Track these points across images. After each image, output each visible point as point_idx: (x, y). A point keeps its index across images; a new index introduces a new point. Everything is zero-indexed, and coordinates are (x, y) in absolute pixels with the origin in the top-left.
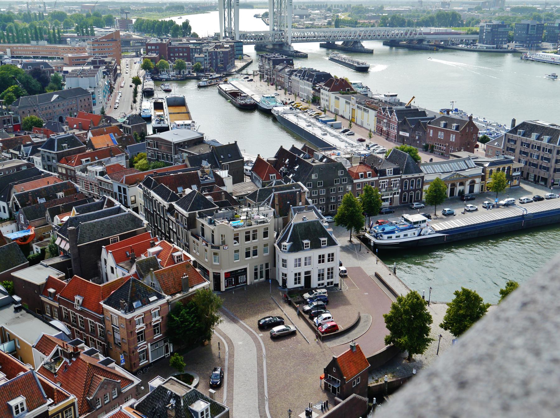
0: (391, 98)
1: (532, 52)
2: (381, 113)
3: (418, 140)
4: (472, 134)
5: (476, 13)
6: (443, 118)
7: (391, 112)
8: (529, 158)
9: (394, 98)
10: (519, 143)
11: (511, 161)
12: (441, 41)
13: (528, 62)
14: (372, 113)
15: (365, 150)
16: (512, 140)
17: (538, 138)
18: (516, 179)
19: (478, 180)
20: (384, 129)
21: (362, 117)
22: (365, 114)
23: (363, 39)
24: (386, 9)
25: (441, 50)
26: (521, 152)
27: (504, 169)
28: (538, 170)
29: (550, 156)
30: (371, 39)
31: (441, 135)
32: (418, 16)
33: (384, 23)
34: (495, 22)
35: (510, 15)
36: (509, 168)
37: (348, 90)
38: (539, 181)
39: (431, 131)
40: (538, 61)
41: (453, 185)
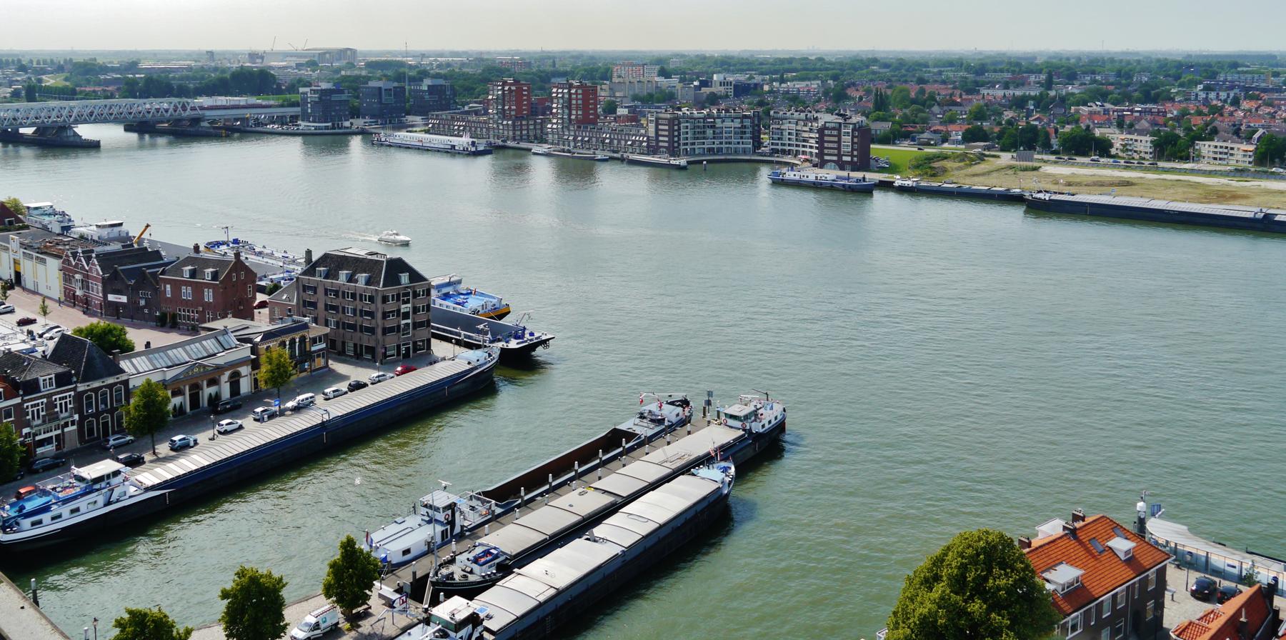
0: (109, 230)
1: (389, 132)
2: (70, 263)
3: (144, 307)
4: (245, 284)
5: (306, 73)
6: (189, 261)
7: (88, 259)
8: (340, 315)
9: (116, 229)
10: (321, 291)
11: (305, 326)
12: (237, 120)
13: (383, 149)
14: (53, 264)
15: (24, 341)
16: (310, 288)
17: (351, 279)
18: (318, 356)
19: (245, 370)
20: (79, 293)
21: (35, 274)
22: (40, 267)
23: (77, 122)
24: (144, 65)
25: (236, 135)
26: (328, 307)
27: (293, 342)
28: (359, 334)
29: (373, 307)
30: (95, 122)
31: (187, 293)
32: (203, 78)
33: (133, 89)
34: (324, 86)
35: (364, 73)
36: (303, 339)
37: (11, 223)
38: (362, 356)
39: (168, 287)
40: (400, 147)
41: (196, 388)
